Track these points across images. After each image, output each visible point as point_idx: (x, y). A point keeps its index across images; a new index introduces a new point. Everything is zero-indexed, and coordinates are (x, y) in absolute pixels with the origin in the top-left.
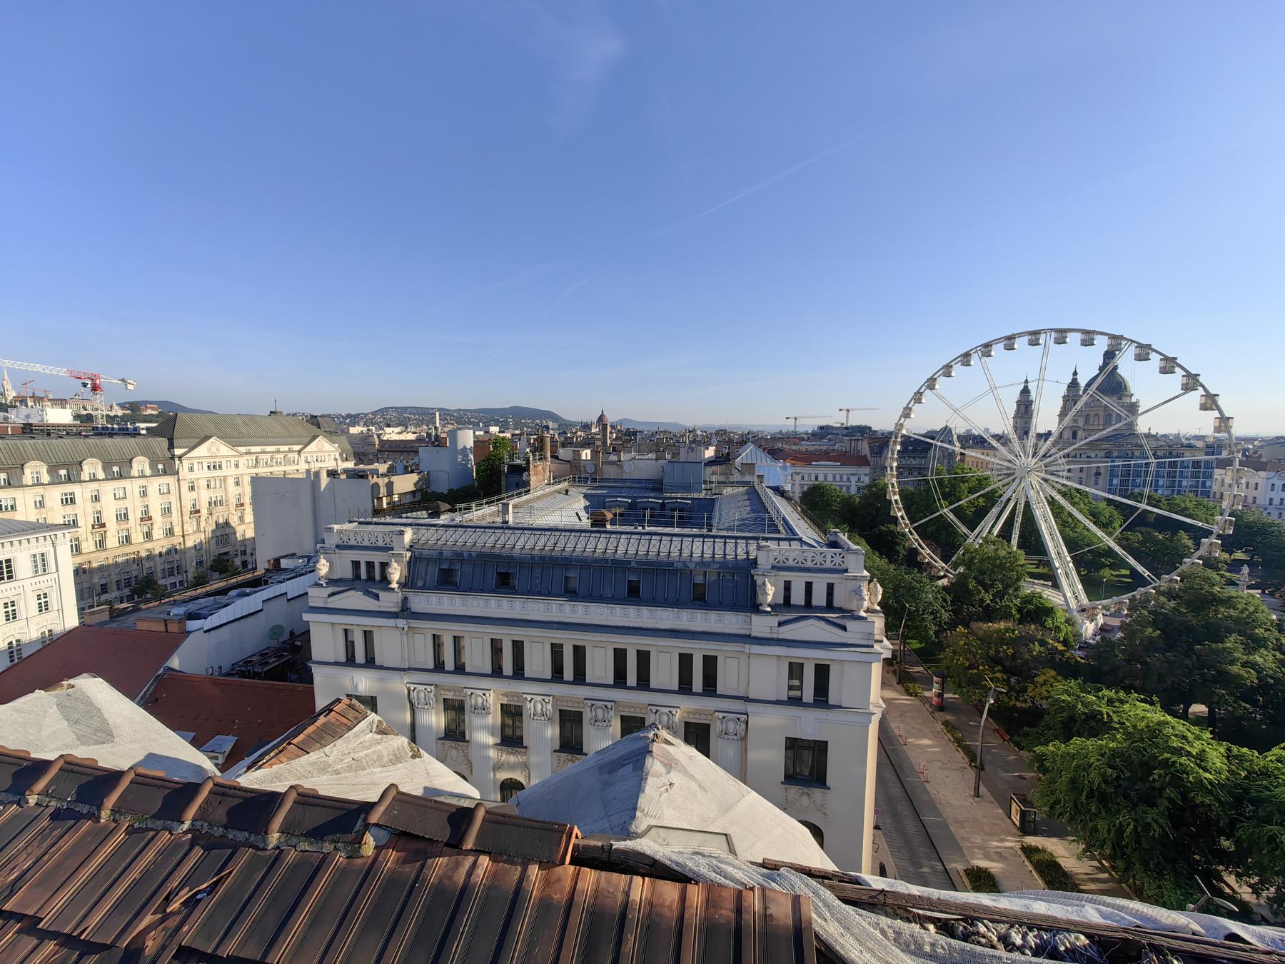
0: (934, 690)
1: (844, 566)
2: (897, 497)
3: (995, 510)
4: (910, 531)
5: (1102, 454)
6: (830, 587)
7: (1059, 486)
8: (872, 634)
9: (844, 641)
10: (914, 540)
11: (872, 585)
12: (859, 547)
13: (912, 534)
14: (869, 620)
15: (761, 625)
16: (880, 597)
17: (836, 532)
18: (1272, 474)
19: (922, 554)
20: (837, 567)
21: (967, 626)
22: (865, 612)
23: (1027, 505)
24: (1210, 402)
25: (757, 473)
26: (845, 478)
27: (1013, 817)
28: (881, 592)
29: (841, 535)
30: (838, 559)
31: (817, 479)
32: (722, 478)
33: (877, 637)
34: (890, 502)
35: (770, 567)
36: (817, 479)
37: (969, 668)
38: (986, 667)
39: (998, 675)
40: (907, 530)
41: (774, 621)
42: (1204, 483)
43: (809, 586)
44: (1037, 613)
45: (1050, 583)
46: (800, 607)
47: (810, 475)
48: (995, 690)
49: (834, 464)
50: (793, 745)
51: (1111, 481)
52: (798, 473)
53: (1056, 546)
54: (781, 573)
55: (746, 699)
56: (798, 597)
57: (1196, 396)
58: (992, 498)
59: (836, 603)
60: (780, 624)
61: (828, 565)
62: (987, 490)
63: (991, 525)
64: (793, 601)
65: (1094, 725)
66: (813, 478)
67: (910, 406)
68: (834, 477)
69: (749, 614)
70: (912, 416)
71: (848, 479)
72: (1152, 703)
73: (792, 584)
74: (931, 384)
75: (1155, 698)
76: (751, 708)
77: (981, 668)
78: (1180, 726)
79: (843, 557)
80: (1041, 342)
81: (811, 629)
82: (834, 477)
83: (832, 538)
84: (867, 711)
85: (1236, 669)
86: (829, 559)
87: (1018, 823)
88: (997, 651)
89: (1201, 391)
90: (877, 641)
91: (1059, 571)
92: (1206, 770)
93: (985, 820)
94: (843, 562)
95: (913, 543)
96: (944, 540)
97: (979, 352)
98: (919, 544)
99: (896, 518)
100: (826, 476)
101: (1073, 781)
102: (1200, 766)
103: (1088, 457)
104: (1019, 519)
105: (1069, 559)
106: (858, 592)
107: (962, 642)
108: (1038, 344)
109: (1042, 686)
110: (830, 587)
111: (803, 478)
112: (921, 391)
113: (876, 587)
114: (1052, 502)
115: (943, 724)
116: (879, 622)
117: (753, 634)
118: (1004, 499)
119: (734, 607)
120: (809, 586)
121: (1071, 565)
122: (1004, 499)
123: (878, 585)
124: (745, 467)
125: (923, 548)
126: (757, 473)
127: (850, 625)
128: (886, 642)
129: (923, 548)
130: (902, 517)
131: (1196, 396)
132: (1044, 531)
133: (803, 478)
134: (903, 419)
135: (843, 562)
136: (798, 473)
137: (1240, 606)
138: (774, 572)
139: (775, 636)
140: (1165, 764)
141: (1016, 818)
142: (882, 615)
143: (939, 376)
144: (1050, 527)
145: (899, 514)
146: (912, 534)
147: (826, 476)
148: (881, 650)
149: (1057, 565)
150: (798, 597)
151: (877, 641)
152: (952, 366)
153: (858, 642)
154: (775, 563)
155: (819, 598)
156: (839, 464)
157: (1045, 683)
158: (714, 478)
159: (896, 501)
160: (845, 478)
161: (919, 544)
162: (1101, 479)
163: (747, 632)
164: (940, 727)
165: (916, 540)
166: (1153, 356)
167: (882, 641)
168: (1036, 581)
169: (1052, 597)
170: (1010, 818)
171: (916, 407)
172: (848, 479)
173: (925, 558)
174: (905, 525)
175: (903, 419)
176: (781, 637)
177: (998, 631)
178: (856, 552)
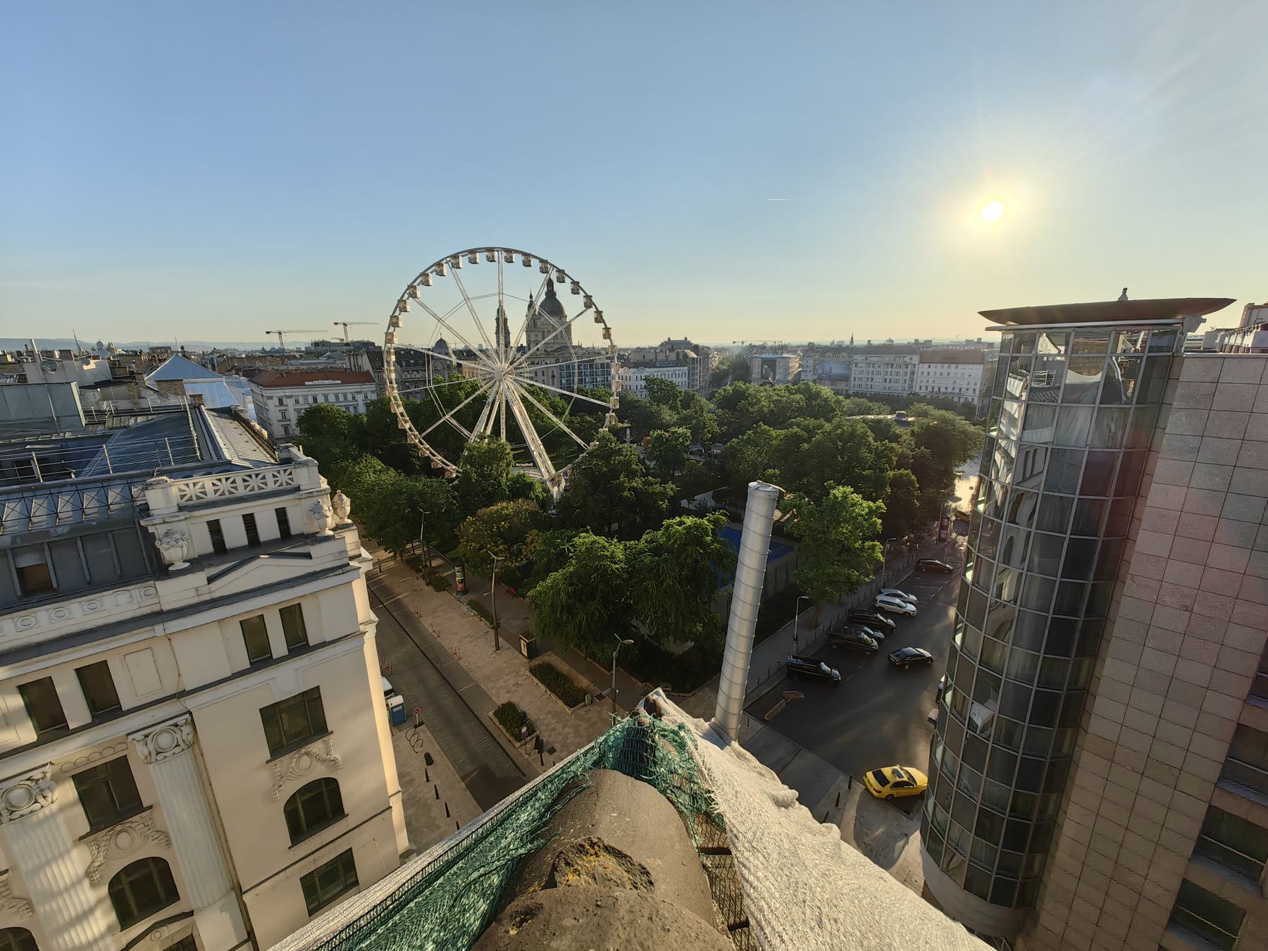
0: (457, 579)
1: (294, 484)
2: (401, 409)
3: (486, 411)
4: (420, 442)
5: (554, 360)
6: (281, 515)
7: (526, 386)
8: (345, 551)
9: (311, 570)
10: (426, 449)
11: (336, 498)
12: (310, 458)
13: (422, 444)
14: (337, 537)
15: (172, 593)
16: (348, 509)
17: (287, 447)
18: (636, 369)
19: (434, 461)
20: (285, 486)
21: (473, 514)
22: (333, 530)
23: (507, 401)
24: (599, 318)
25: (189, 393)
26: (349, 397)
27: (523, 652)
28: (349, 503)
29: (294, 450)
30: (283, 478)
31: (315, 400)
32: (124, 405)
33: (351, 554)
34: (396, 414)
35: (176, 509)
36: (315, 400)
37: (481, 548)
38: (492, 544)
39: (501, 547)
40: (417, 441)
41: (200, 578)
42: (607, 378)
43: (249, 521)
44: (522, 489)
45: (531, 464)
46: (241, 549)
47: (305, 397)
48: (497, 560)
49: (333, 382)
50: (270, 715)
51: (561, 380)
52: (290, 397)
53: (531, 434)
54: (197, 513)
55: (182, 694)
56: (235, 535)
57: (591, 313)
58: (482, 400)
59: (295, 528)
60: (211, 580)
61: (271, 486)
62: (478, 392)
63: (483, 426)
64: (229, 544)
65: (560, 559)
66: (311, 400)
67: (397, 314)
68: (337, 397)
69: (151, 583)
70: (401, 324)
71: (354, 398)
72: (587, 532)
73: (221, 521)
74: (411, 291)
75: (588, 527)
76: (190, 703)
77: (489, 546)
78: (601, 540)
79: (290, 474)
80: (496, 259)
81: (264, 570)
82: (337, 397)
83: (284, 455)
84: (358, 633)
85: (626, 493)
86: (270, 480)
87: (526, 654)
88: (498, 528)
89: (593, 309)
90: (352, 558)
91: (535, 453)
92: (615, 563)
93: (505, 665)
94: (292, 479)
95: (424, 452)
96: (449, 443)
97: (450, 263)
98: (431, 453)
99: (404, 431)
100: (326, 397)
101: (552, 606)
102: (611, 562)
103: (546, 363)
104: (503, 417)
105: (540, 442)
106: (317, 511)
107: (472, 530)
108: (494, 261)
109: (531, 544)
110: (281, 515)
111: (297, 402)
112: (404, 299)
113: (342, 500)
114: (524, 399)
115: (467, 604)
116: (351, 538)
117: (166, 608)
118: (490, 400)
119: (121, 580)
120: (249, 521)
121: (542, 447)
122: (490, 400)
123: (344, 496)
124: (164, 385)
125: (434, 456)
126: (189, 393)
127: (315, 550)
128: (365, 554)
129: (434, 456)
130: (410, 429)
131: (591, 313)
132: (521, 423)
133: (297, 402)
134: (392, 329)
135: (292, 479)
136: (290, 397)
137: (624, 453)
138: (183, 515)
139: (207, 597)
140: (597, 569)
141: (525, 652)
142: (355, 527)
143: (418, 285)
144: (524, 419)
145: (407, 426)
146: (422, 444)
147: (326, 397)
148: (359, 565)
149: (533, 449)
150: (235, 535)
151: (352, 558)
152: (428, 275)
153: (329, 566)
154: (183, 502)
155: (268, 529)
156: (339, 382)
157: (532, 542)
158: (105, 406)
159: (402, 414)
160: (349, 397)
161: (431, 453)
162: (555, 380)
163: (156, 608)
164: (465, 608)
165: (427, 449)
166: (567, 279)
167: (360, 555)
168: (523, 465)
169: (532, 475)
170: (521, 653)
171: (402, 316)
172: (354, 398)
173: (438, 464)
174: (415, 438)
175: (392, 329)
176: (216, 595)
177: (497, 511)
178: (305, 464)
